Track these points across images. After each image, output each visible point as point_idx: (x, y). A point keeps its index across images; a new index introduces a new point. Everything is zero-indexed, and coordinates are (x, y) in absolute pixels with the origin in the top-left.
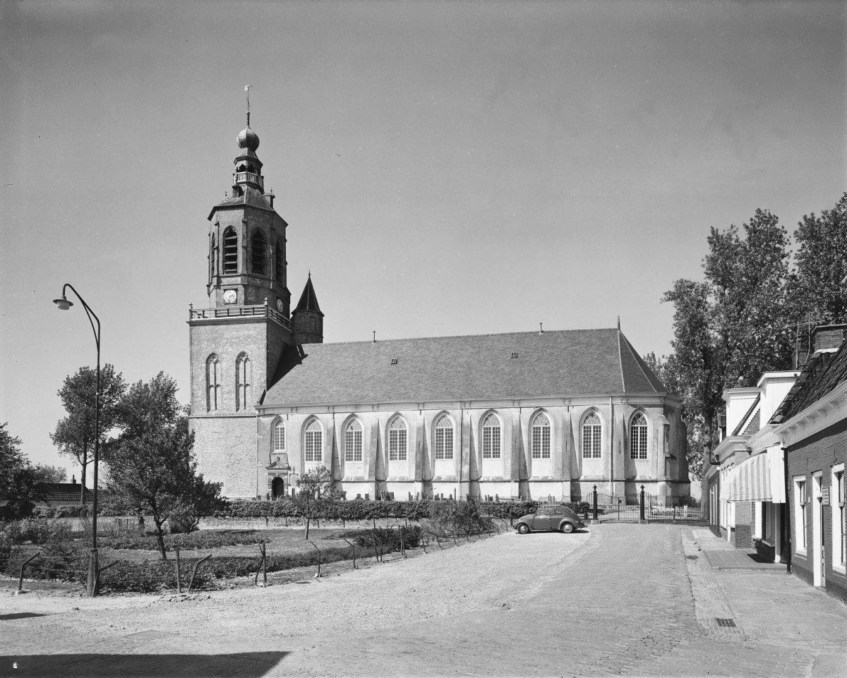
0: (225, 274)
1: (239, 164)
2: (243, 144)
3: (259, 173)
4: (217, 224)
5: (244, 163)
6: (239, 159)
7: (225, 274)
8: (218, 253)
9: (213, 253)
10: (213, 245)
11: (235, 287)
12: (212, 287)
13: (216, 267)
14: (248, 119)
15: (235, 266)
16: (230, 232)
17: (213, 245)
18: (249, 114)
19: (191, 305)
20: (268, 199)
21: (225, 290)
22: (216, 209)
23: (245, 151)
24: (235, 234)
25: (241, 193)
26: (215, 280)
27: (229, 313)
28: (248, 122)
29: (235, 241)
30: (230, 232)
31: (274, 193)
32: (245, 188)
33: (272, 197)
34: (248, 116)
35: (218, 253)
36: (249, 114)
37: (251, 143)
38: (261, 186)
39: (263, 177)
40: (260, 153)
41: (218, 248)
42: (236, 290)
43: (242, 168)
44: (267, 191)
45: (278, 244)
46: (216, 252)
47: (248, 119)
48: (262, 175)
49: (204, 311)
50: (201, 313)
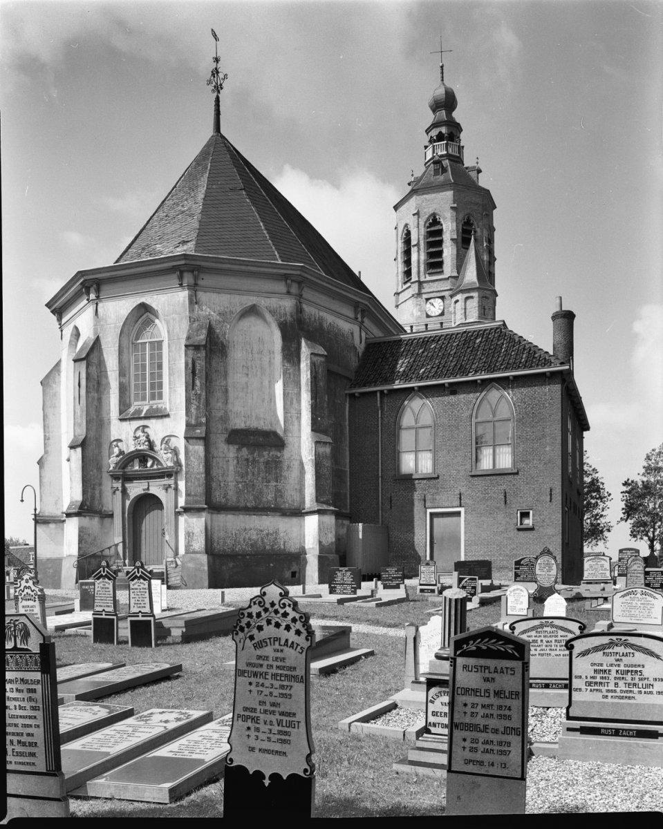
0: (429, 278)
1: (434, 133)
2: (436, 106)
5: (444, 130)
7: (429, 278)
11: (442, 294)
14: (442, 73)
15: (440, 264)
16: (434, 221)
21: (427, 300)
23: (443, 114)
28: (443, 77)
29: (440, 232)
32: (446, 163)
34: (442, 69)
36: (442, 67)
37: (447, 103)
39: (463, 147)
42: (443, 298)
43: (440, 137)
47: (442, 73)
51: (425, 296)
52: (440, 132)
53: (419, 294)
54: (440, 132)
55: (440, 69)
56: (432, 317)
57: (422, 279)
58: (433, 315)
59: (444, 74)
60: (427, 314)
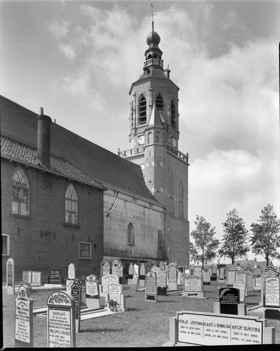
0: (140, 126)
1: (148, 55)
3: (160, 58)
4: (135, 95)
5: (151, 53)
6: (147, 52)
7: (140, 126)
8: (135, 114)
9: (132, 114)
10: (132, 109)
12: (132, 136)
13: (134, 123)
14: (153, 26)
16: (143, 98)
17: (132, 109)
18: (153, 23)
19: (119, 149)
20: (166, 73)
21: (139, 136)
22: (134, 84)
24: (145, 99)
25: (149, 72)
26: (134, 130)
27: (138, 151)
30: (143, 98)
31: (170, 69)
32: (151, 69)
33: (169, 72)
35: (135, 114)
36: (153, 23)
38: (162, 67)
40: (160, 46)
41: (135, 110)
43: (150, 57)
44: (165, 68)
45: (172, 102)
46: (134, 112)
47: (153, 26)
48: (162, 60)
49: (125, 152)
50: (124, 153)
51: (138, 135)
52: (150, 55)
53: (135, 134)
54: (150, 55)
55: (152, 24)
56: (141, 145)
57: (137, 127)
58: (141, 144)
59: (154, 27)
60: (139, 144)
